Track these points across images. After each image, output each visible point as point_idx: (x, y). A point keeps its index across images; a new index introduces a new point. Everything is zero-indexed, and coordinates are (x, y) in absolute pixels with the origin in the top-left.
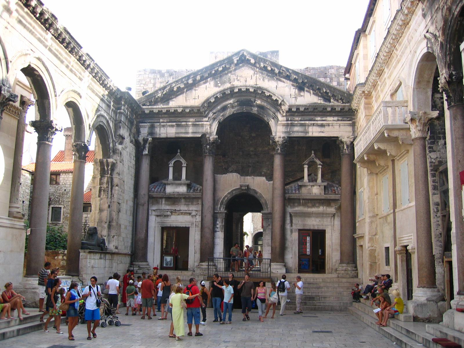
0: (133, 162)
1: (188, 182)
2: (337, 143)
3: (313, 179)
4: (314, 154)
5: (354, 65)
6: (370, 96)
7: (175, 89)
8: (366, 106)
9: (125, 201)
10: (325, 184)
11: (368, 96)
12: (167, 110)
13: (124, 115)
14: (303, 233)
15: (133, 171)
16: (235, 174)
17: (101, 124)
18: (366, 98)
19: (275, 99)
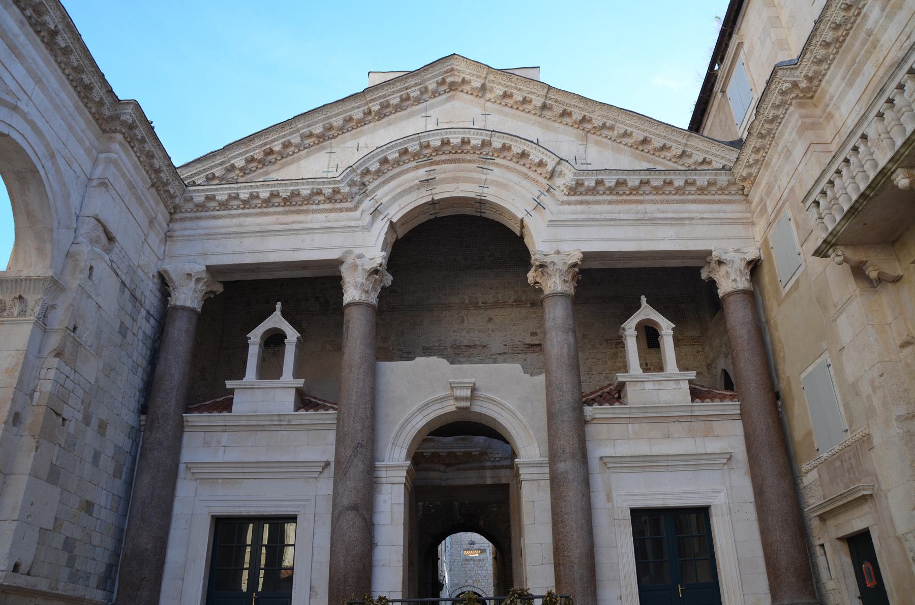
0: (146, 327)
1: (300, 383)
2: (704, 275)
3: (652, 364)
4: (647, 302)
5: (720, 95)
6: (812, 98)
7: (277, 147)
8: (807, 120)
9: (94, 422)
10: (692, 375)
11: (808, 92)
12: (251, 194)
13: (123, 175)
14: (645, 521)
16: (435, 358)
18: (801, 106)
19: (537, 160)
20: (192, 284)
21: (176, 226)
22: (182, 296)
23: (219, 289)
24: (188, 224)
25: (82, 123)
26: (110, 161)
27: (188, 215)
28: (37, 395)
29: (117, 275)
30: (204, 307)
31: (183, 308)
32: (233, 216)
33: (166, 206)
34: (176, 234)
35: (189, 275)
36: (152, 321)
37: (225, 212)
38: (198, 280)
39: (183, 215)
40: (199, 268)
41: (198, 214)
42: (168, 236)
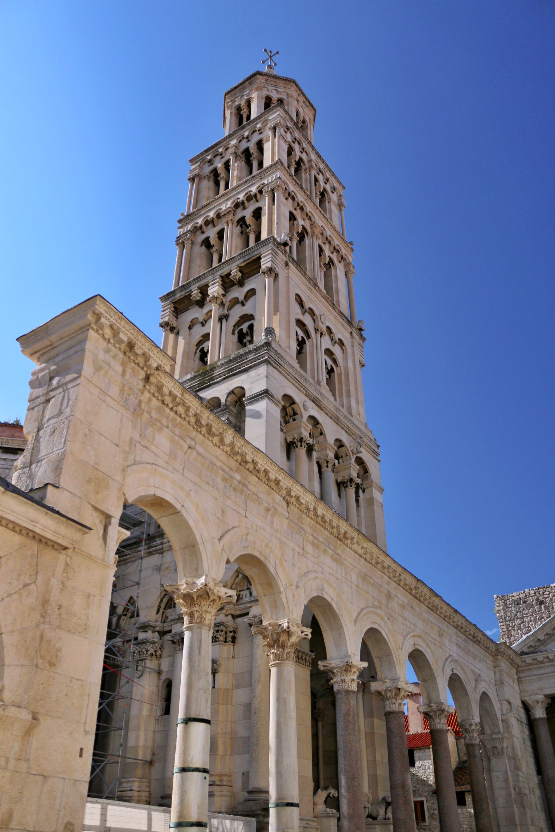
0: (527, 731)
15: (528, 743)
17: (484, 690)
20: (540, 705)
21: (522, 675)
22: (537, 712)
23: (549, 701)
24: (527, 674)
25: (489, 660)
26: (501, 671)
27: (525, 668)
28: (517, 788)
29: (516, 717)
30: (547, 714)
31: (541, 719)
32: (548, 666)
33: (514, 667)
34: (523, 679)
35: (538, 702)
36: (527, 727)
37: (543, 665)
38: (542, 702)
39: (522, 669)
40: (540, 697)
41: (530, 667)
42: (519, 680)
